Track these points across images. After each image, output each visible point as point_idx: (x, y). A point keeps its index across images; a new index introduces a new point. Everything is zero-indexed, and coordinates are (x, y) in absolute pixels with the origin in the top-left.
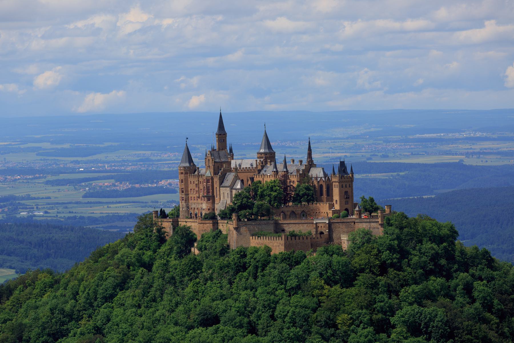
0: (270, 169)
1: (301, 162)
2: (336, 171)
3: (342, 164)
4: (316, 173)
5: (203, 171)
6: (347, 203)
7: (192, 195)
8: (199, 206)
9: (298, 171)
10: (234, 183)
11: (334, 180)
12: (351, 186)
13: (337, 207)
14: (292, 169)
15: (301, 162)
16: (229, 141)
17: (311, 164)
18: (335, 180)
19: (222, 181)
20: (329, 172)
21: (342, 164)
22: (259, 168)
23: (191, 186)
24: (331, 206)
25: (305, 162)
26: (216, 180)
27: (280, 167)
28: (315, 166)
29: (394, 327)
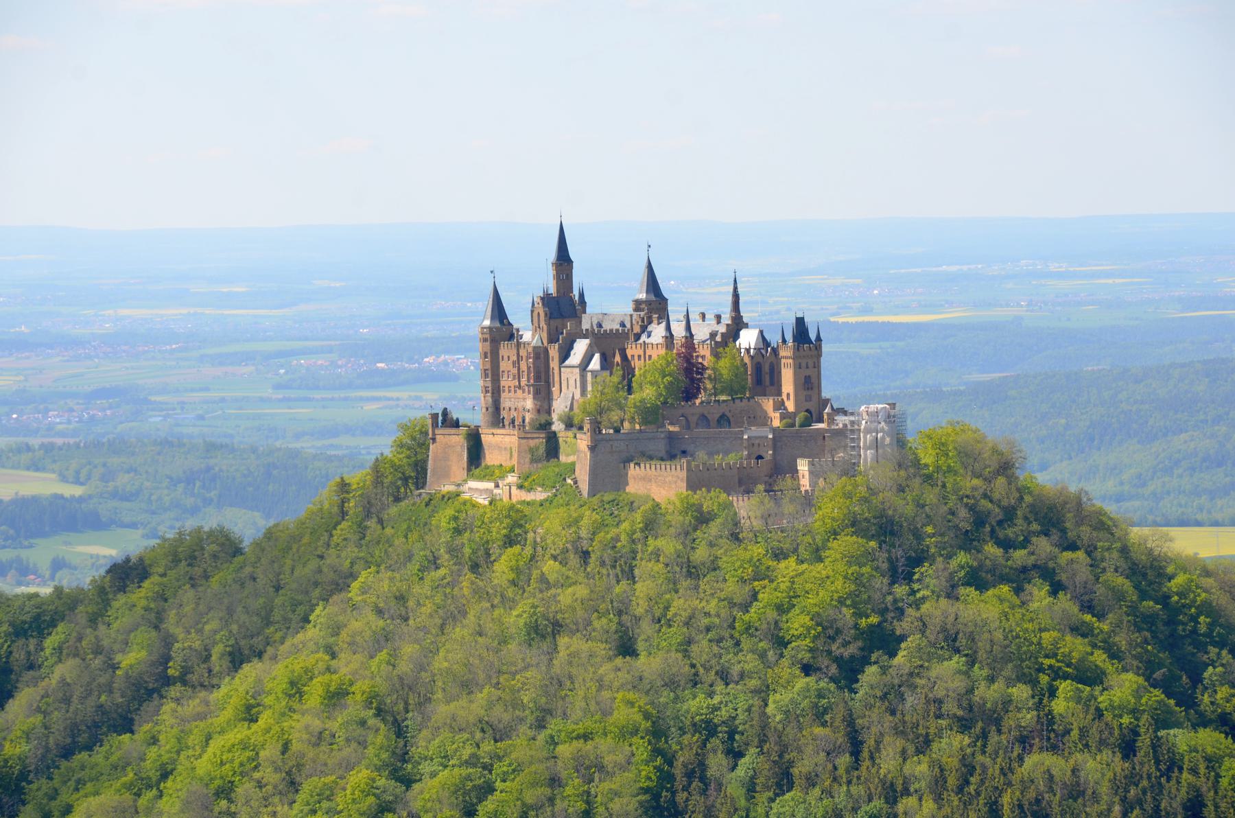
0: (657, 332)
1: (718, 318)
2: (789, 337)
3: (800, 322)
4: (748, 339)
5: (527, 336)
6: (808, 399)
7: (506, 382)
8: (520, 405)
9: (713, 335)
10: (587, 359)
11: (782, 353)
12: (817, 366)
13: (790, 406)
14: (701, 332)
15: (718, 318)
16: (579, 278)
17: (738, 324)
18: (786, 352)
19: (565, 354)
20: (774, 339)
21: (800, 322)
22: (637, 329)
23: (504, 365)
24: (780, 406)
25: (727, 319)
26: (554, 352)
27: (679, 330)
28: (746, 326)
29: (903, 638)
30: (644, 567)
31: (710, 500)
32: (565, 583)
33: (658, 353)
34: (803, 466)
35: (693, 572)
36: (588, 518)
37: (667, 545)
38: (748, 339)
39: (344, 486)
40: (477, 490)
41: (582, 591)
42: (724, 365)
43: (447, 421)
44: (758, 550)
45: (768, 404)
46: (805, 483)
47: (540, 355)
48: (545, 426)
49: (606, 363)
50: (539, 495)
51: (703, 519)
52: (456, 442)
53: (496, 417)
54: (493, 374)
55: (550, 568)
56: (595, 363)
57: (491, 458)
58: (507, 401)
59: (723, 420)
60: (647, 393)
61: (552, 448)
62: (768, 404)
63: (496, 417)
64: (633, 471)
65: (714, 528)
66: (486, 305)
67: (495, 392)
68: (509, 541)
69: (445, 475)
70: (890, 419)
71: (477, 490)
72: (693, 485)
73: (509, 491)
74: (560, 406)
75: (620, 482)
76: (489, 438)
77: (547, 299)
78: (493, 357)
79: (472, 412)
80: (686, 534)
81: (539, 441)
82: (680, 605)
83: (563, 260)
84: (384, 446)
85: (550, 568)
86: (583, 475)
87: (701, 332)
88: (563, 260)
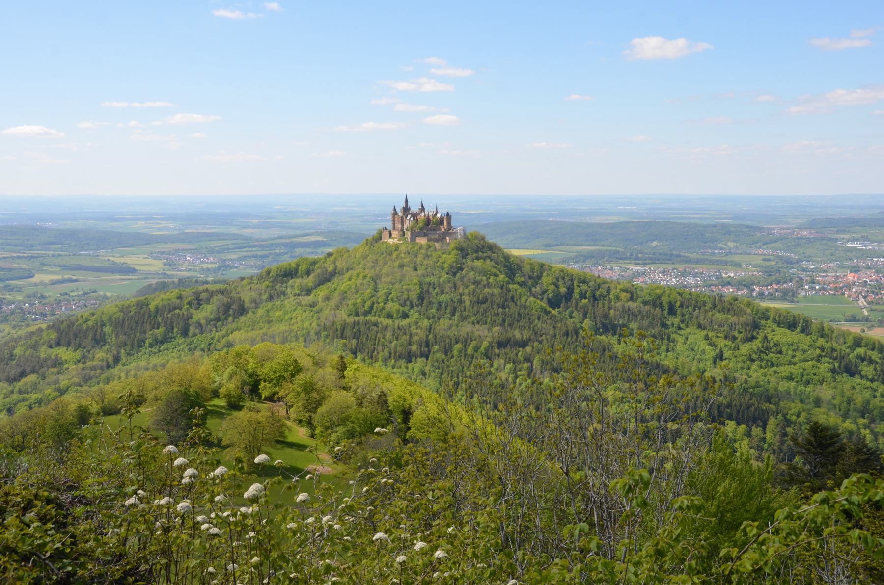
0: (423, 214)
4: (439, 215)
14: (430, 214)
17: (437, 213)
19: (406, 217)
27: (427, 214)
30: (419, 255)
31: (431, 244)
32: (405, 258)
33: (423, 218)
34: (448, 238)
35: (428, 256)
36: (410, 246)
37: (423, 251)
38: (439, 215)
39: (367, 240)
40: (391, 241)
41: (408, 259)
42: (434, 220)
43: (386, 229)
44: (439, 253)
45: (442, 227)
46: (448, 241)
47: (402, 218)
48: (402, 230)
49: (414, 219)
50: (401, 242)
51: (430, 247)
52: (387, 232)
53: (394, 229)
54: (394, 221)
55: (403, 255)
56: (412, 219)
57: (393, 236)
58: (396, 226)
59: (434, 230)
60: (421, 225)
61: (404, 234)
62: (442, 227)
63: (394, 229)
64: (417, 238)
65: (432, 249)
66: (393, 208)
67: (394, 224)
68: (396, 250)
69: (385, 238)
70: (463, 230)
71: (391, 241)
72: (428, 241)
73: (396, 241)
74: (405, 227)
75: (415, 240)
76: (393, 232)
77: (403, 208)
78: (394, 217)
79: (389, 225)
80: (427, 250)
81: (401, 233)
82: (425, 262)
83: (407, 201)
84: (375, 233)
85: (403, 255)
86: (409, 239)
87: (430, 214)
88: (407, 201)
